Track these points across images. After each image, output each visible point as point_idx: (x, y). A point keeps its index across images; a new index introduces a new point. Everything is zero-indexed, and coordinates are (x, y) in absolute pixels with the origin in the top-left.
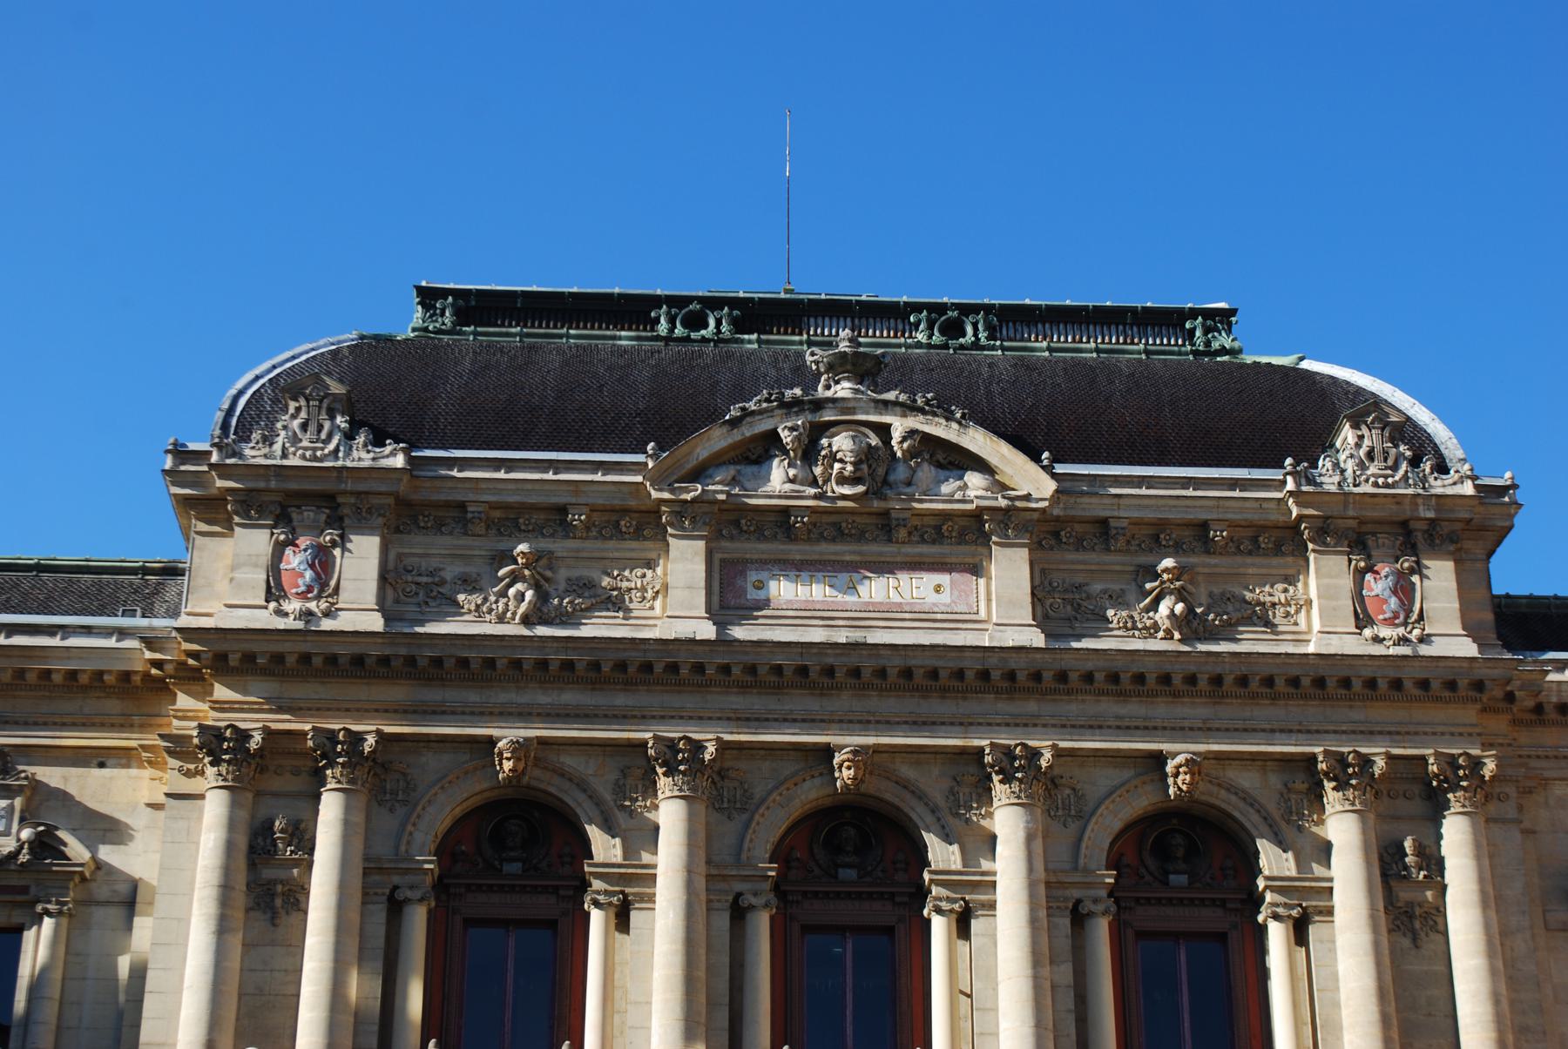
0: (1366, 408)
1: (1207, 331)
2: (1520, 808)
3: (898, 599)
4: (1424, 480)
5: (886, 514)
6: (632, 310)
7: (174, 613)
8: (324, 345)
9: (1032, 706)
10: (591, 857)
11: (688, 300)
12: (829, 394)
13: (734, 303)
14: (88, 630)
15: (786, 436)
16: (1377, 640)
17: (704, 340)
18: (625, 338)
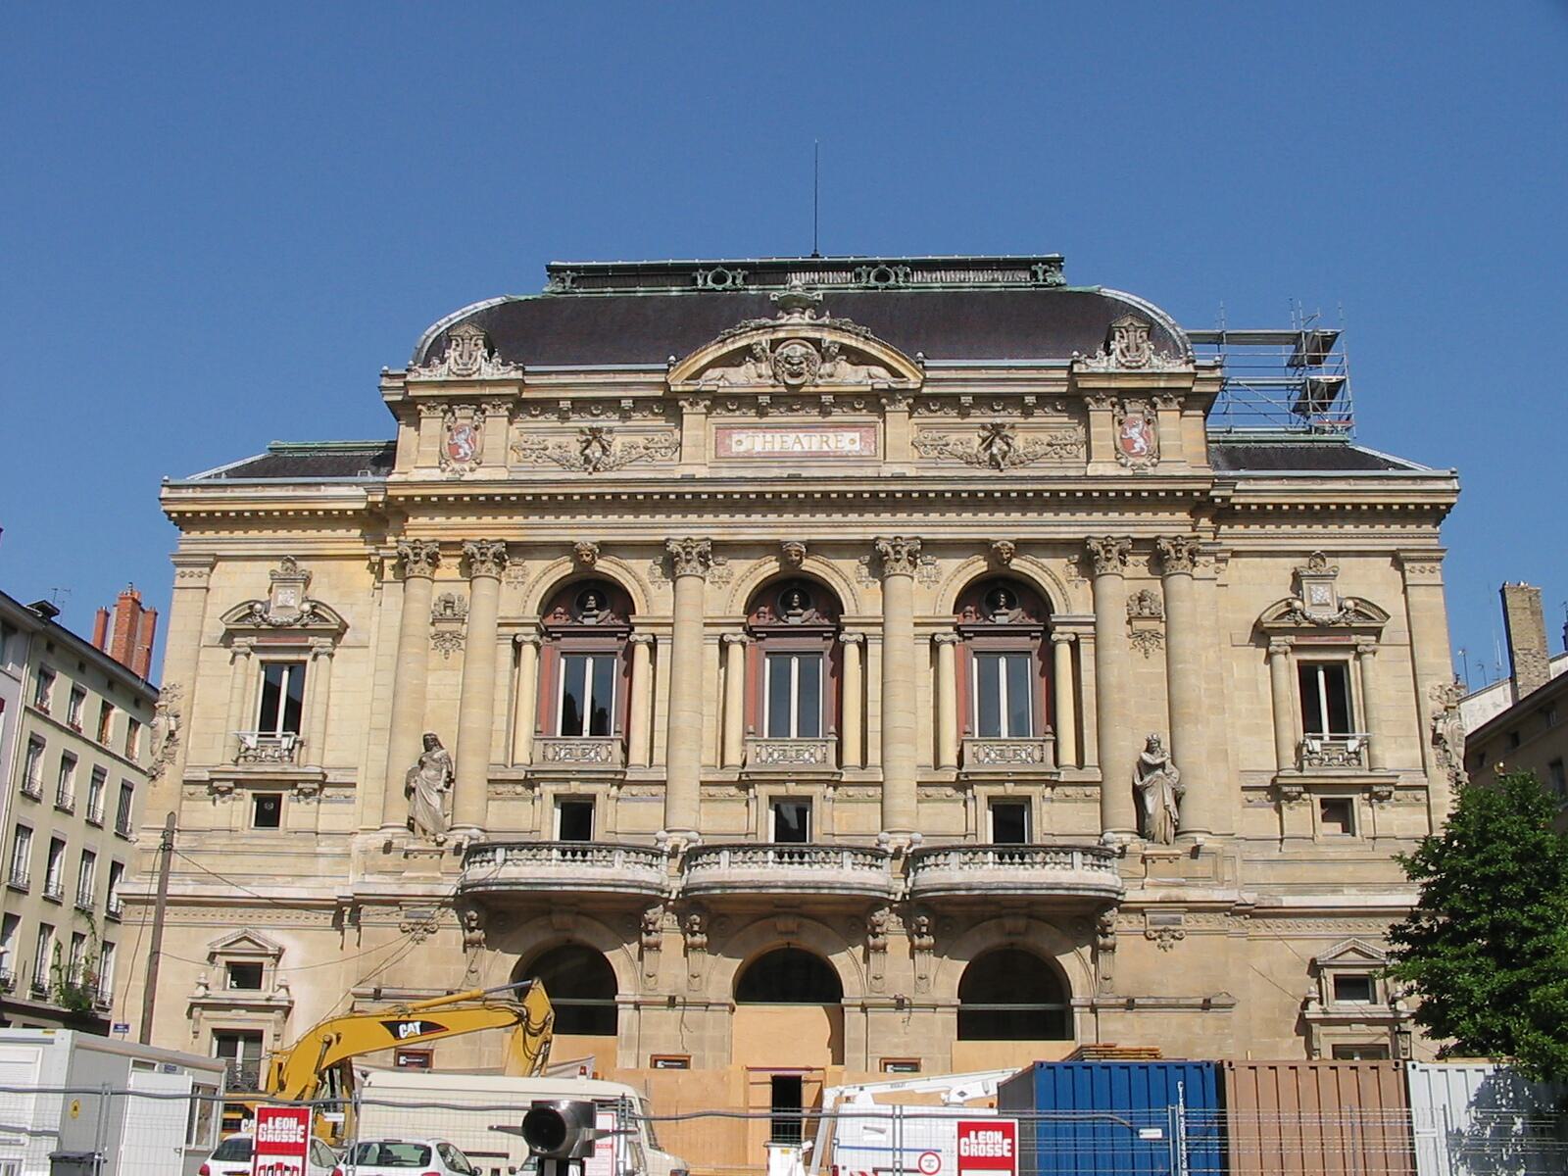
1: (1045, 271)
3: (826, 448)
5: (819, 395)
6: (683, 273)
7: (389, 474)
8: (482, 305)
10: (634, 613)
11: (715, 266)
12: (782, 321)
13: (744, 266)
14: (338, 484)
17: (725, 290)
18: (675, 291)
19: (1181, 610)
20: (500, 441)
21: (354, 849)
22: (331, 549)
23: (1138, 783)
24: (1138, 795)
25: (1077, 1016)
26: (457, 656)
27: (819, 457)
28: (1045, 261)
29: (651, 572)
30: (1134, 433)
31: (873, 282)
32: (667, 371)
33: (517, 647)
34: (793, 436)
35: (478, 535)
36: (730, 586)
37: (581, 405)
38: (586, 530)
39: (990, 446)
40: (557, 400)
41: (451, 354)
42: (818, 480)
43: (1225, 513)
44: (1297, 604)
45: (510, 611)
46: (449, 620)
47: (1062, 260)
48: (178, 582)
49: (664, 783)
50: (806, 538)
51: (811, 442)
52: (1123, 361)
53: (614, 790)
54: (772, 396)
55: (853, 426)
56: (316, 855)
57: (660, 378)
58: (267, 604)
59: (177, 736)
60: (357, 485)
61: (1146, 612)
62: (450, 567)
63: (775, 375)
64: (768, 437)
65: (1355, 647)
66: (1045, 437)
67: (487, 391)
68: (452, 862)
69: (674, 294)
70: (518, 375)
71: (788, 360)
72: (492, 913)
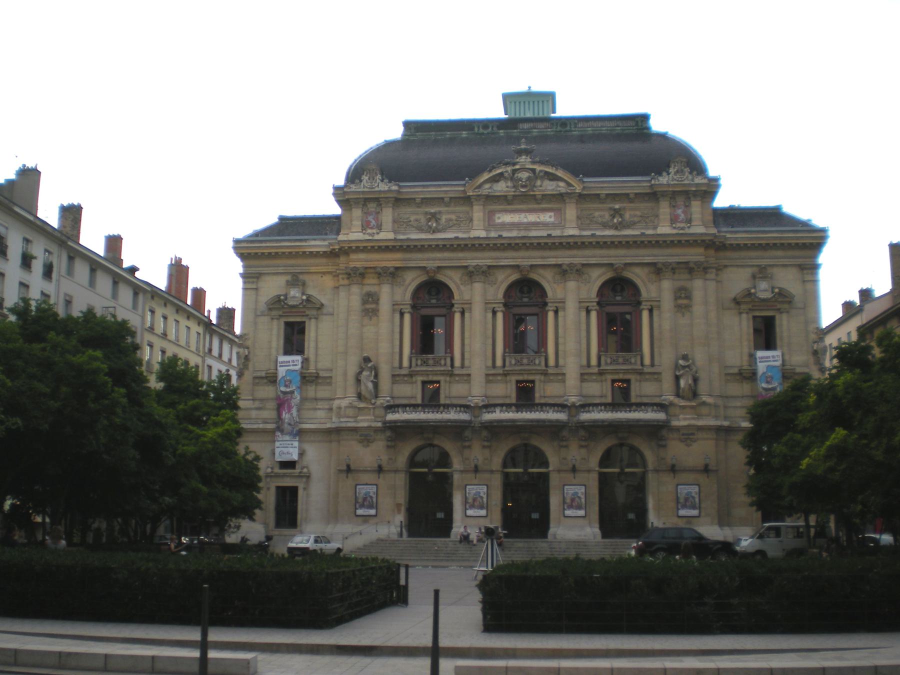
2: (717, 275)
4: (693, 180)
5: (535, 195)
7: (338, 233)
9: (575, 252)
14: (315, 240)
15: (506, 175)
16: (675, 228)
18: (464, 134)
19: (698, 295)
20: (390, 219)
21: (334, 406)
22: (313, 269)
24: (677, 378)
26: (374, 319)
29: (461, 280)
30: (679, 212)
31: (559, 128)
32: (464, 185)
33: (402, 314)
37: (426, 201)
38: (431, 261)
39: (614, 217)
40: (414, 199)
41: (365, 178)
44: (753, 291)
45: (398, 298)
46: (371, 303)
49: (469, 375)
51: (532, 218)
53: (448, 379)
54: (514, 196)
56: (316, 409)
57: (462, 189)
58: (286, 296)
59: (251, 356)
60: (324, 240)
61: (683, 295)
63: (514, 187)
64: (512, 215)
65: (779, 309)
66: (638, 213)
68: (380, 412)
70: (395, 188)
71: (520, 179)
72: (397, 432)
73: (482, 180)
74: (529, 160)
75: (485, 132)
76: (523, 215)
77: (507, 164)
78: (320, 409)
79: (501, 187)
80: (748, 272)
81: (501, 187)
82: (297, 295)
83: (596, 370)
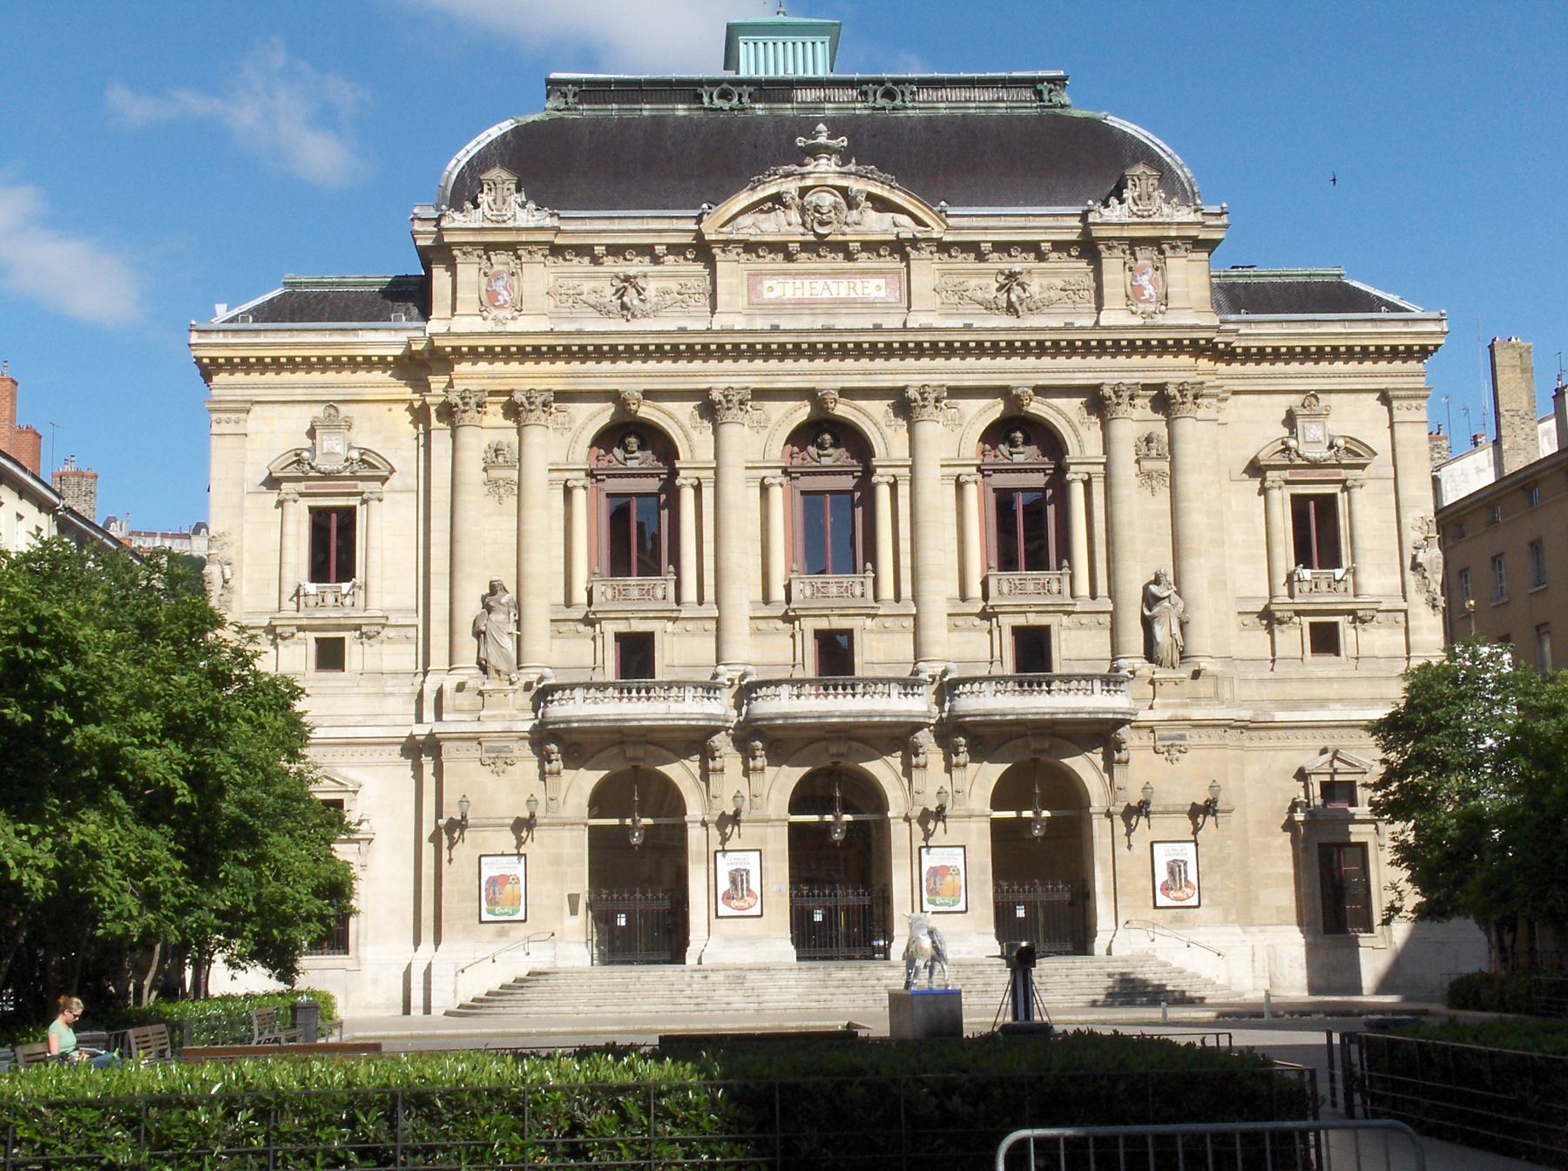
0: (1145, 154)
3: (853, 295)
5: (846, 243)
8: (494, 132)
12: (809, 168)
14: (375, 329)
15: (787, 198)
17: (732, 109)
18: (681, 110)
22: (370, 394)
23: (1147, 613)
24: (1147, 624)
25: (1095, 823)
27: (848, 303)
28: (1051, 80)
34: (821, 282)
35: (528, 384)
36: (767, 431)
41: (485, 198)
42: (851, 331)
43: (1228, 355)
44: (1292, 443)
47: (1064, 79)
48: (216, 429)
50: (840, 385)
51: (840, 289)
52: (1135, 209)
53: (669, 626)
54: (801, 243)
55: (878, 273)
56: (385, 695)
57: (692, 225)
61: (1154, 452)
62: (494, 413)
63: (804, 224)
64: (798, 282)
65: (1343, 482)
67: (523, 238)
69: (681, 113)
73: (736, 209)
74: (834, 168)
75: (726, 106)
76: (820, 283)
77: (787, 175)
78: (392, 694)
79: (773, 226)
80: (1279, 406)
81: (773, 226)
82: (338, 449)
83: (978, 606)
